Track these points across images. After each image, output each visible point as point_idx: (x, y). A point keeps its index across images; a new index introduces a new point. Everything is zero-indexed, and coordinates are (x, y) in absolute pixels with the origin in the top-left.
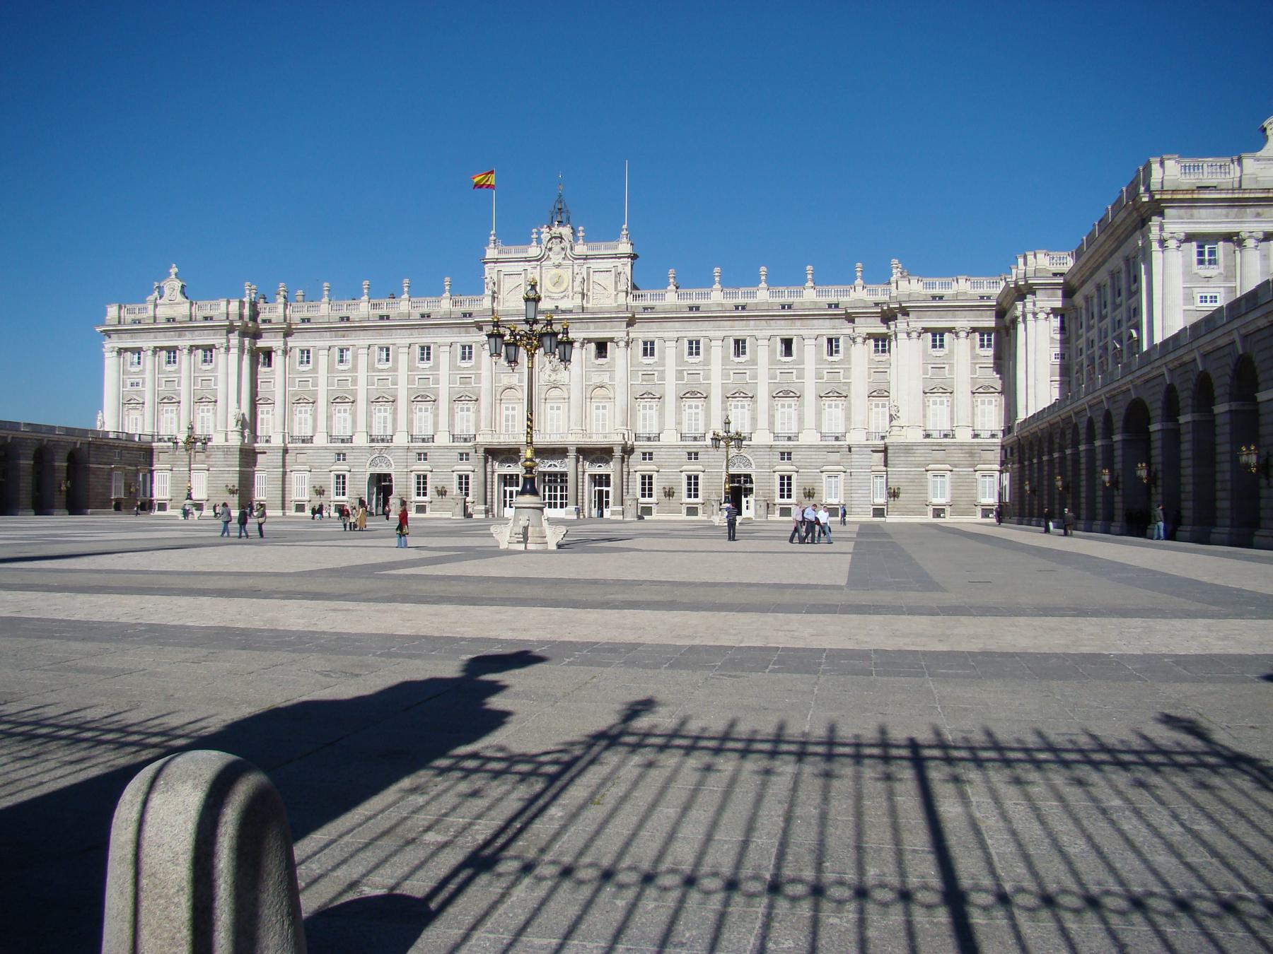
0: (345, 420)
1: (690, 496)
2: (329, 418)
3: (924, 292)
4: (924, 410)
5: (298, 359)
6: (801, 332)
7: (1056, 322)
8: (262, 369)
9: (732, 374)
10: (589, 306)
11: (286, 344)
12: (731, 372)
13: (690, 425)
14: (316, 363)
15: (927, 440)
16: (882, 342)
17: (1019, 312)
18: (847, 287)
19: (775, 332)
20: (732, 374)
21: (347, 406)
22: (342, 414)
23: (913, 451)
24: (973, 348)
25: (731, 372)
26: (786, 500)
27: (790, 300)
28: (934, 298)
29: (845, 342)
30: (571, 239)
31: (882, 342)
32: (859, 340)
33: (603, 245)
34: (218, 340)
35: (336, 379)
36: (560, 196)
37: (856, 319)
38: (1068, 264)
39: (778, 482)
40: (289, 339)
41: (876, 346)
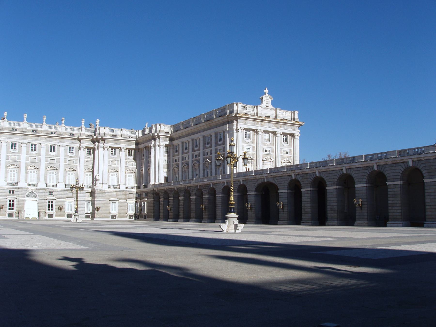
1: (9, 209)
3: (109, 133)
4: (108, 178)
6: (59, 144)
7: (165, 149)
9: (30, 158)
12: (30, 158)
13: (11, 179)
15: (110, 189)
16: (91, 150)
17: (153, 144)
18: (78, 128)
19: (49, 143)
20: (30, 158)
23: (105, 193)
24: (126, 155)
25: (30, 158)
26: (50, 211)
27: (55, 130)
28: (113, 136)
29: (76, 149)
31: (91, 150)
37: (81, 141)
39: (48, 204)
41: (88, 151)
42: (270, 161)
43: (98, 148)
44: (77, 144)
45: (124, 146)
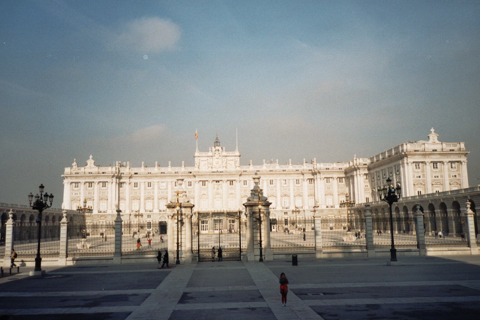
2: (145, 204)
5: (134, 186)
8: (121, 189)
10: (227, 170)
11: (130, 181)
12: (269, 190)
14: (140, 187)
15: (327, 208)
21: (151, 201)
22: (149, 203)
24: (338, 182)
30: (221, 150)
32: (305, 180)
33: (231, 152)
34: (109, 180)
35: (147, 192)
36: (217, 138)
38: (368, 162)
40: (131, 179)
41: (310, 182)
42: (440, 184)
43: (316, 179)
44: (302, 177)
45: (335, 176)
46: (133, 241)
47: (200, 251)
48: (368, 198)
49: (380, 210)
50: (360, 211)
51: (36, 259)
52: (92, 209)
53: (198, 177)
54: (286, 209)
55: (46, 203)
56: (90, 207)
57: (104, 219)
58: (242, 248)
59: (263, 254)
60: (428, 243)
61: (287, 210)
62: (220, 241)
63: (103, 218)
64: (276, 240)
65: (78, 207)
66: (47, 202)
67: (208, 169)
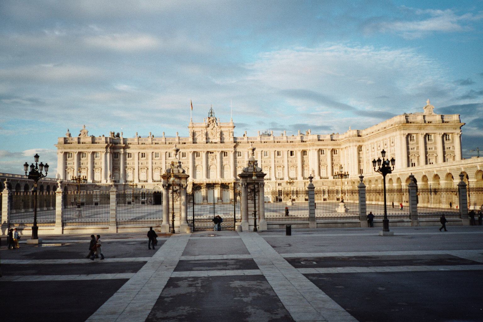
0: (144, 175)
10: (222, 141)
14: (134, 157)
46: (128, 210)
47: (195, 221)
48: (362, 170)
49: (373, 182)
50: (354, 183)
51: (33, 228)
52: (86, 179)
53: (192, 148)
54: (280, 181)
55: (41, 173)
56: (85, 177)
57: (98, 189)
58: (236, 218)
59: (257, 224)
60: (420, 214)
61: (282, 181)
62: (215, 211)
63: (97, 188)
64: (270, 210)
65: (73, 177)
66: (42, 171)
67: (202, 140)
